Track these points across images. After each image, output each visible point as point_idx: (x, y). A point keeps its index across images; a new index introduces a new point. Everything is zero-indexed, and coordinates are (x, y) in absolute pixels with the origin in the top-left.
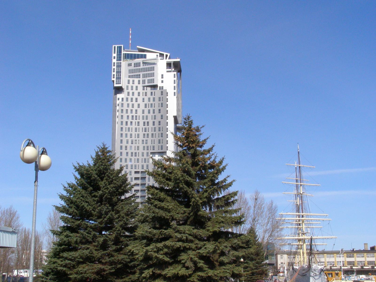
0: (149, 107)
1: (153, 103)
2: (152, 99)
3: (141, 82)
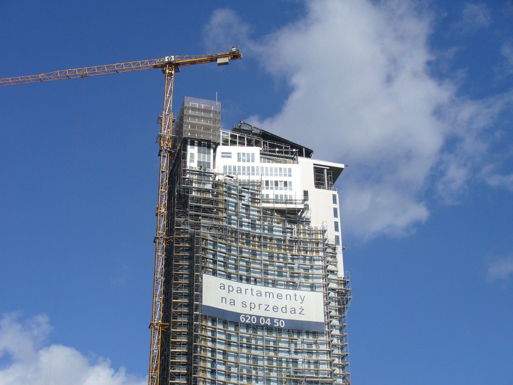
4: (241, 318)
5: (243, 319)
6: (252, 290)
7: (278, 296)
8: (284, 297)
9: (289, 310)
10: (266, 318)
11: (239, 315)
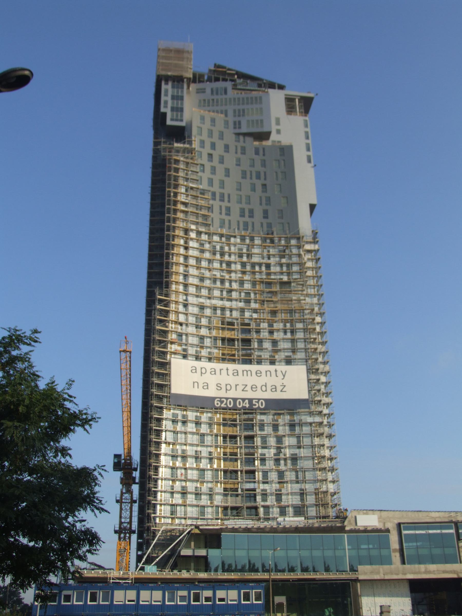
0: (251, 178)
1: (262, 170)
2: (258, 163)
3: (231, 125)
4: (216, 402)
5: (218, 404)
6: (227, 369)
7: (256, 373)
8: (264, 373)
9: (269, 388)
10: (244, 400)
11: (213, 399)
